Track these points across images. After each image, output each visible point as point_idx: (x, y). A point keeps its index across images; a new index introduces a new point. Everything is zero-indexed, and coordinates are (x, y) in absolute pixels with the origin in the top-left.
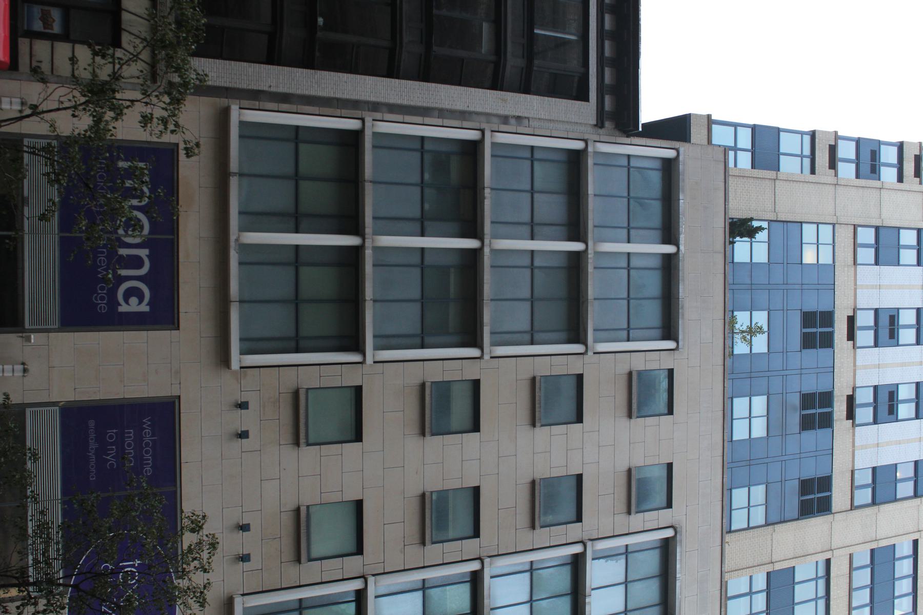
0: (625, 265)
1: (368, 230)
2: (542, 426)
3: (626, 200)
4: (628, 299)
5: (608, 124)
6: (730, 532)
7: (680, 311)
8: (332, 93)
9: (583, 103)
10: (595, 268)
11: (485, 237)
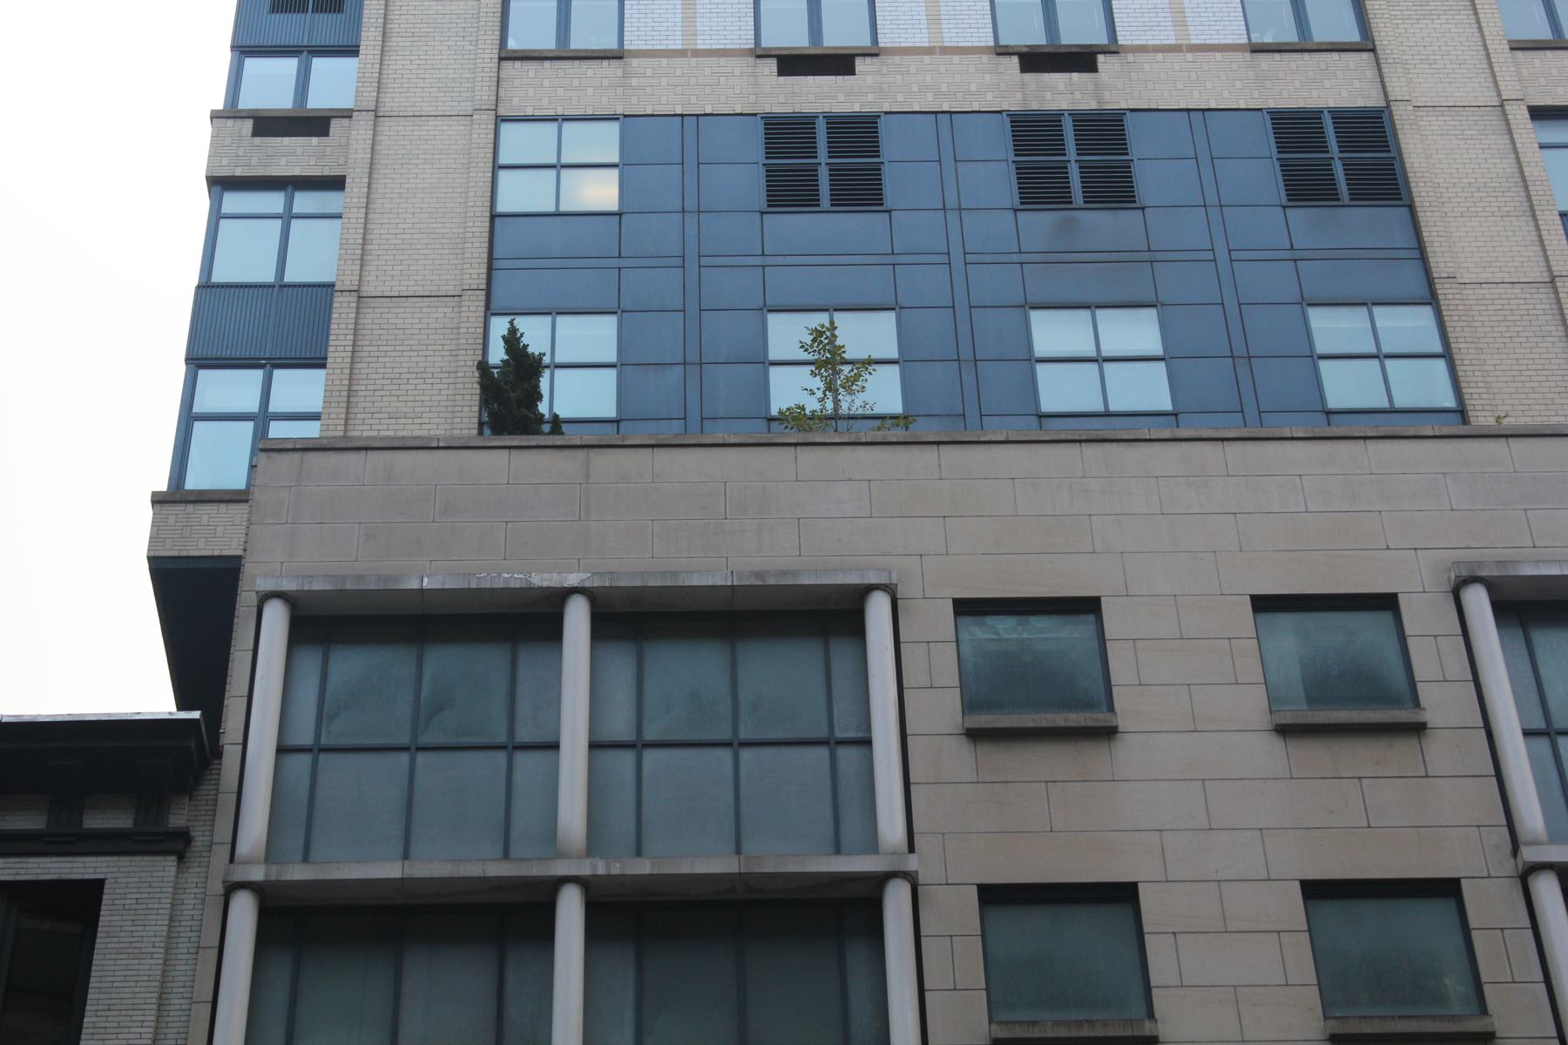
0: (628, 757)
2: (1151, 1015)
3: (421, 758)
4: (735, 745)
5: (177, 819)
6: (1461, 412)
7: (772, 581)
9: (106, 898)
10: (639, 853)
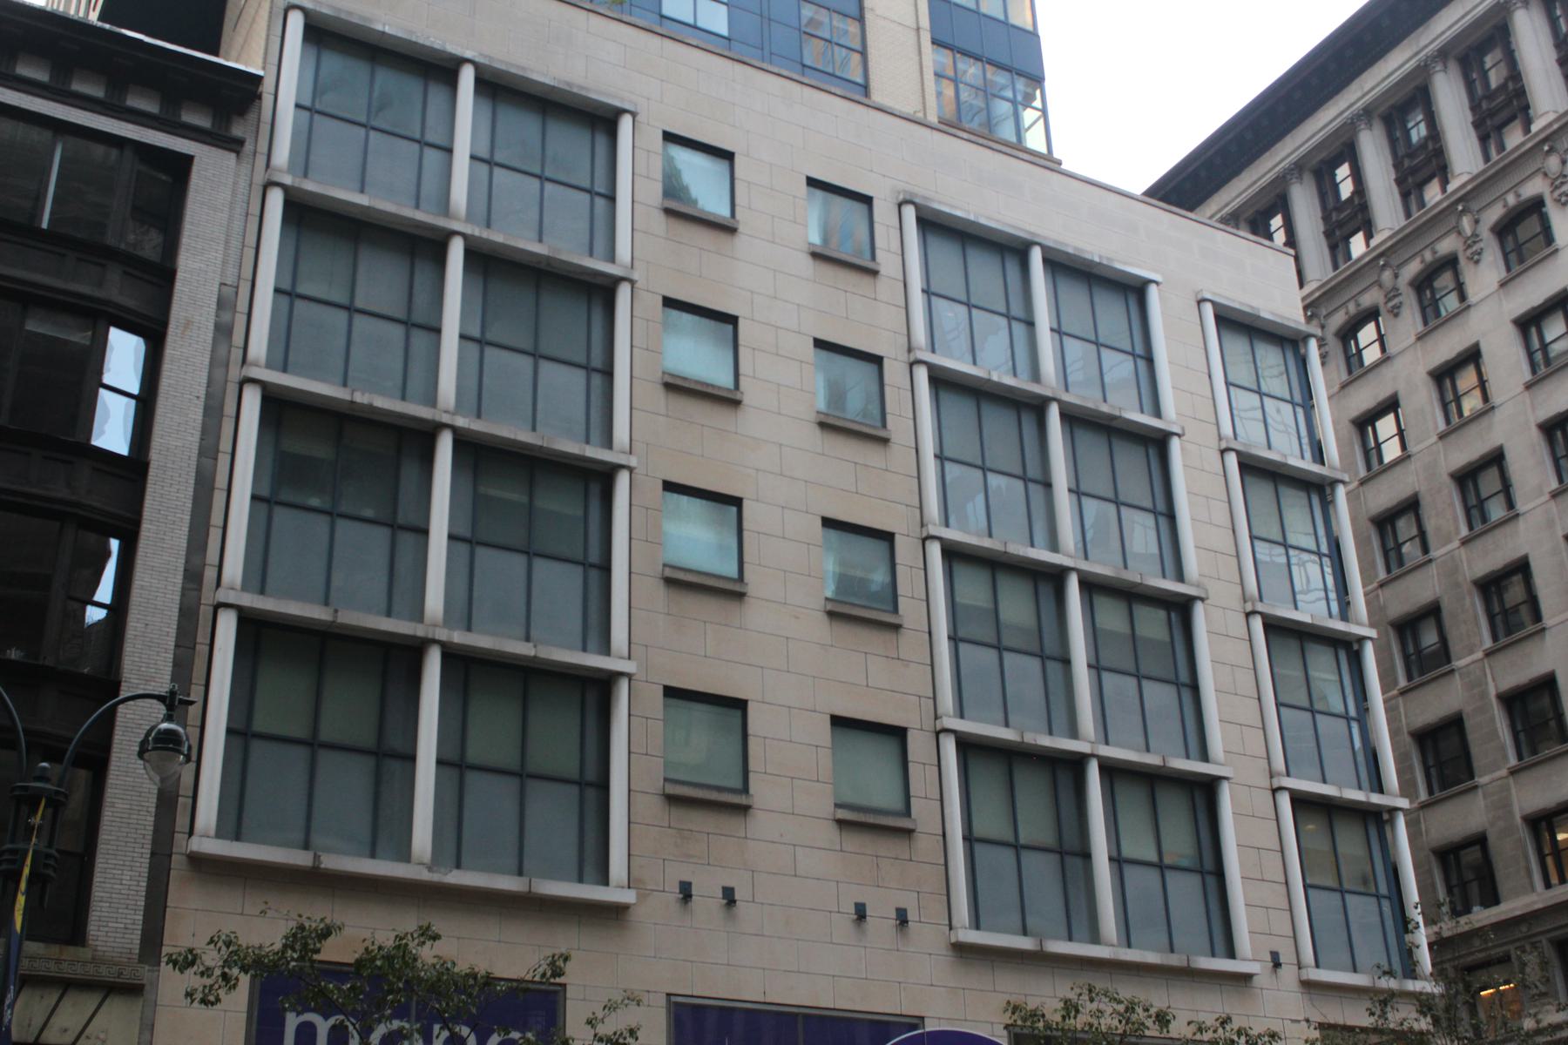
1: (420, 631)
5: (237, 131)
6: (866, 88)
8: (167, 655)
9: (195, 169)
11: (437, 418)
